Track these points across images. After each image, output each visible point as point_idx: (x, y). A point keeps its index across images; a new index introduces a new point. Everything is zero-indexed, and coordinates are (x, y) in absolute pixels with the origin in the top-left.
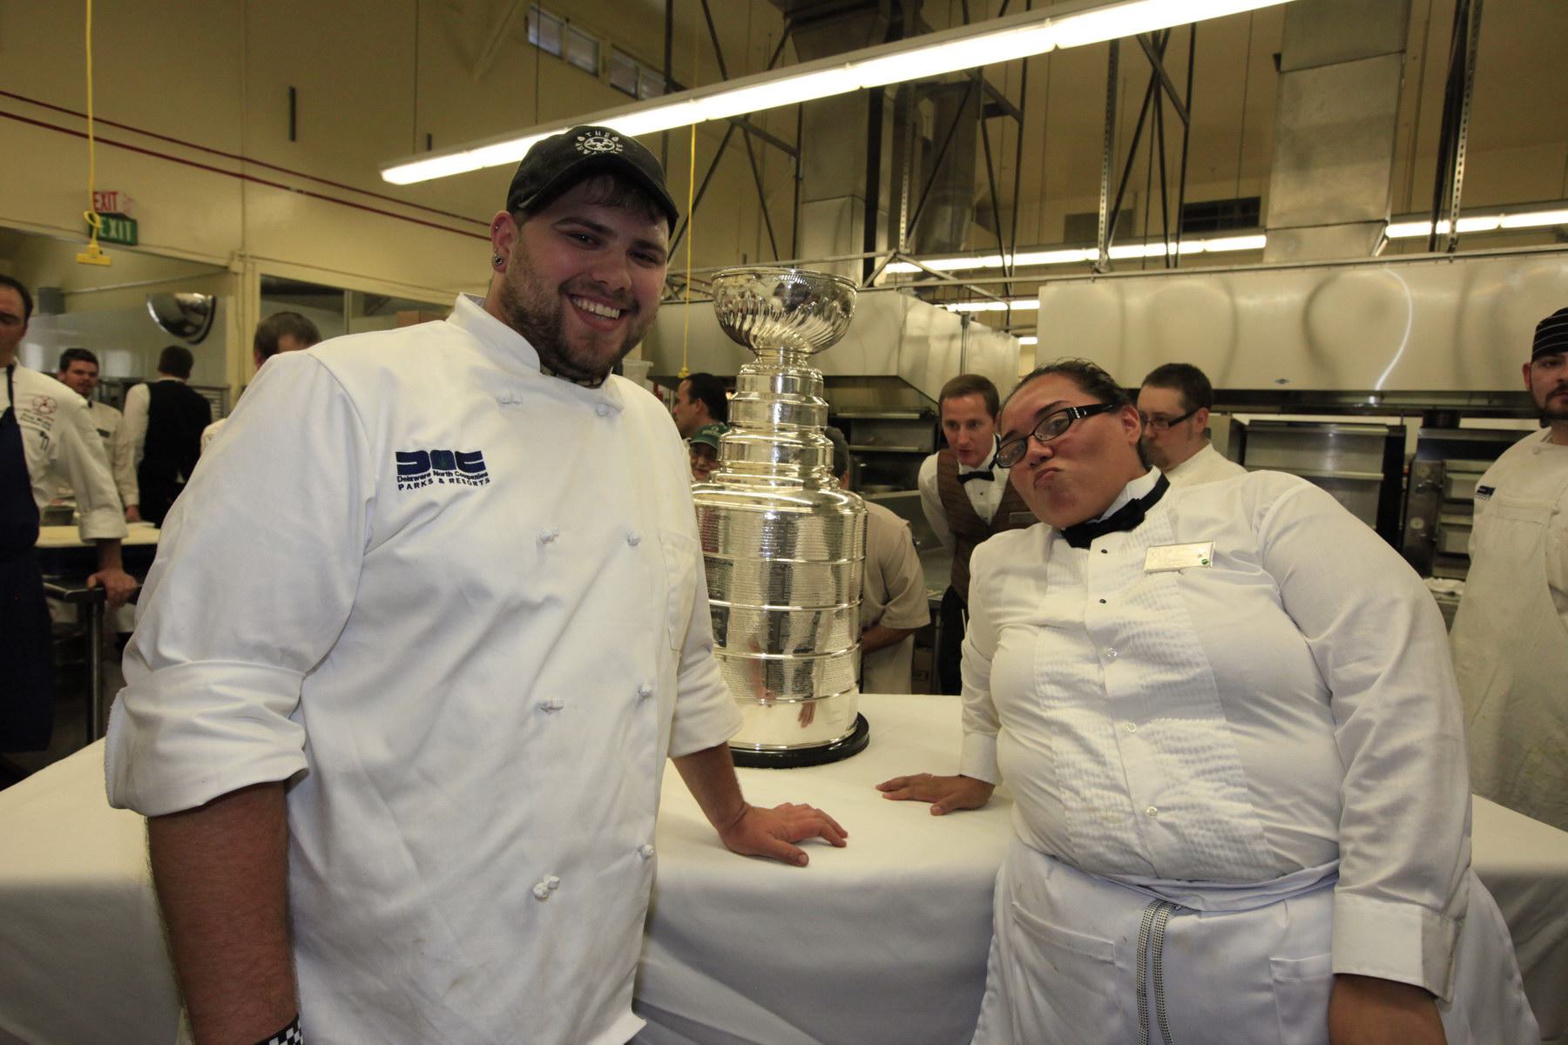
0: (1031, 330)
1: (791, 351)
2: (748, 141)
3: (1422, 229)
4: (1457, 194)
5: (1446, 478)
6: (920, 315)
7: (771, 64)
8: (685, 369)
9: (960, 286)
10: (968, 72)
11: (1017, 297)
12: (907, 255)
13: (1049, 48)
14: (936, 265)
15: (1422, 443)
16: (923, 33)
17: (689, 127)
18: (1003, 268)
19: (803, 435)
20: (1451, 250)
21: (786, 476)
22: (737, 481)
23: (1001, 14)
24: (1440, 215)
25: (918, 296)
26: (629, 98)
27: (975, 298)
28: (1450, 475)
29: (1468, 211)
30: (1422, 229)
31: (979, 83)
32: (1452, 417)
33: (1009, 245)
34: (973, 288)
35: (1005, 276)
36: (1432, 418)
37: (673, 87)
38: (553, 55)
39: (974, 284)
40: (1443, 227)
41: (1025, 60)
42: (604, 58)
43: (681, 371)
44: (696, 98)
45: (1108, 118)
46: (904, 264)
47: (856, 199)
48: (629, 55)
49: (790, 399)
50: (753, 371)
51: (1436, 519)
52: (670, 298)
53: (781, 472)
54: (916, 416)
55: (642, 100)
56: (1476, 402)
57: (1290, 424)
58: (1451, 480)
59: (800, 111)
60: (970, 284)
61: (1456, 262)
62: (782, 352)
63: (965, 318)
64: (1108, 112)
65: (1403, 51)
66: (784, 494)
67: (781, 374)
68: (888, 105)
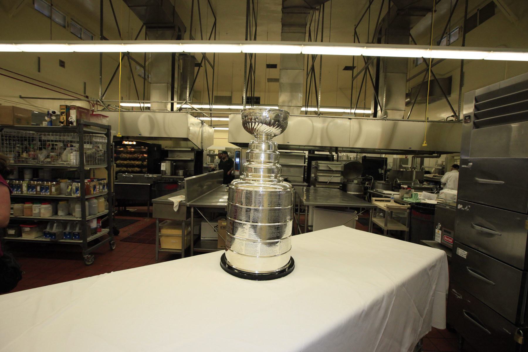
0: (227, 126)
1: (269, 137)
2: (129, 61)
3: (303, 109)
4: (319, 103)
5: (318, 165)
6: (192, 120)
7: (136, 38)
8: (119, 134)
9: (201, 113)
10: (202, 53)
11: (213, 117)
12: (189, 103)
13: (240, 52)
14: (196, 106)
15: (309, 157)
16: (192, 40)
17: (119, 53)
18: (210, 108)
19: (275, 164)
20: (319, 115)
21: (270, 178)
22: (255, 181)
23: (209, 39)
24: (308, 106)
25: (191, 115)
26: (79, 39)
27: (204, 116)
28: (319, 164)
29: (321, 107)
30: (303, 109)
31: (205, 57)
32: (314, 151)
33: (211, 102)
34: (204, 114)
35: (210, 111)
36: (311, 151)
37: (103, 38)
38: (45, 15)
39: (204, 113)
40: (310, 109)
41: (214, 53)
42: (67, 22)
43: (117, 134)
44: (124, 44)
45: (245, 73)
46: (188, 105)
47: (169, 84)
48: (78, 24)
49: (268, 152)
50: (257, 142)
51: (316, 174)
52: (104, 109)
53: (269, 177)
54: (190, 149)
55: (84, 40)
56: (316, 148)
57: (286, 152)
58: (319, 166)
59: (145, 55)
60: (203, 113)
61: (321, 118)
62: (264, 136)
63: (202, 122)
64: (245, 71)
65: (304, 70)
66: (268, 184)
67: (264, 143)
68: (176, 58)
